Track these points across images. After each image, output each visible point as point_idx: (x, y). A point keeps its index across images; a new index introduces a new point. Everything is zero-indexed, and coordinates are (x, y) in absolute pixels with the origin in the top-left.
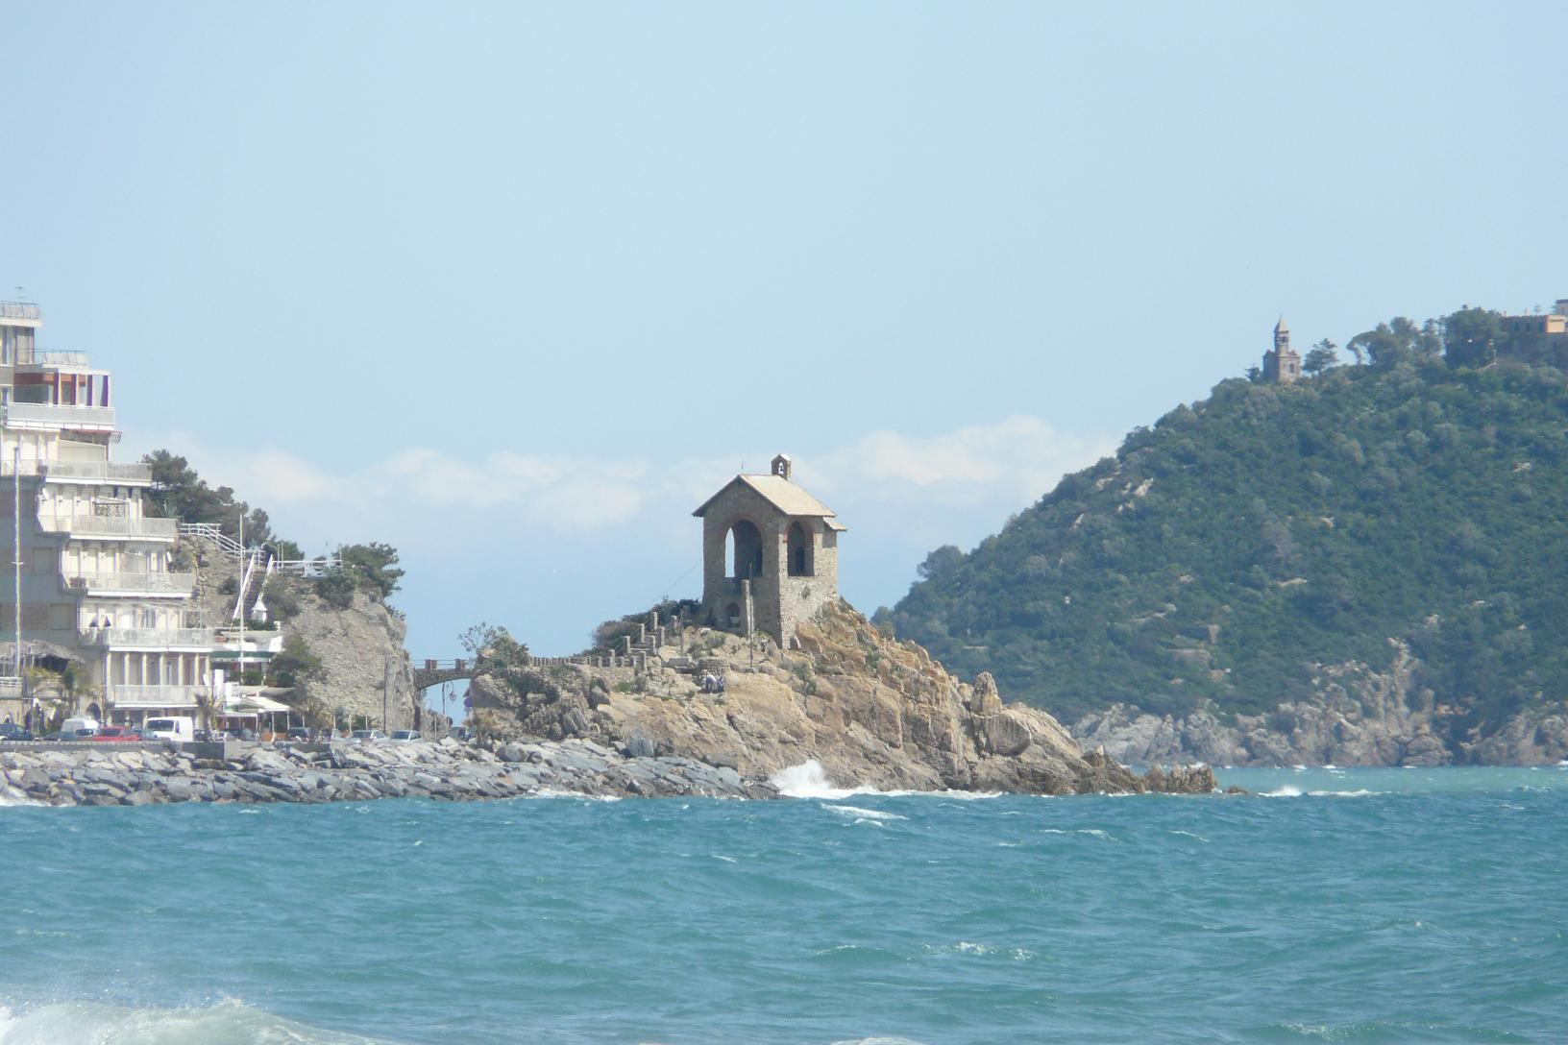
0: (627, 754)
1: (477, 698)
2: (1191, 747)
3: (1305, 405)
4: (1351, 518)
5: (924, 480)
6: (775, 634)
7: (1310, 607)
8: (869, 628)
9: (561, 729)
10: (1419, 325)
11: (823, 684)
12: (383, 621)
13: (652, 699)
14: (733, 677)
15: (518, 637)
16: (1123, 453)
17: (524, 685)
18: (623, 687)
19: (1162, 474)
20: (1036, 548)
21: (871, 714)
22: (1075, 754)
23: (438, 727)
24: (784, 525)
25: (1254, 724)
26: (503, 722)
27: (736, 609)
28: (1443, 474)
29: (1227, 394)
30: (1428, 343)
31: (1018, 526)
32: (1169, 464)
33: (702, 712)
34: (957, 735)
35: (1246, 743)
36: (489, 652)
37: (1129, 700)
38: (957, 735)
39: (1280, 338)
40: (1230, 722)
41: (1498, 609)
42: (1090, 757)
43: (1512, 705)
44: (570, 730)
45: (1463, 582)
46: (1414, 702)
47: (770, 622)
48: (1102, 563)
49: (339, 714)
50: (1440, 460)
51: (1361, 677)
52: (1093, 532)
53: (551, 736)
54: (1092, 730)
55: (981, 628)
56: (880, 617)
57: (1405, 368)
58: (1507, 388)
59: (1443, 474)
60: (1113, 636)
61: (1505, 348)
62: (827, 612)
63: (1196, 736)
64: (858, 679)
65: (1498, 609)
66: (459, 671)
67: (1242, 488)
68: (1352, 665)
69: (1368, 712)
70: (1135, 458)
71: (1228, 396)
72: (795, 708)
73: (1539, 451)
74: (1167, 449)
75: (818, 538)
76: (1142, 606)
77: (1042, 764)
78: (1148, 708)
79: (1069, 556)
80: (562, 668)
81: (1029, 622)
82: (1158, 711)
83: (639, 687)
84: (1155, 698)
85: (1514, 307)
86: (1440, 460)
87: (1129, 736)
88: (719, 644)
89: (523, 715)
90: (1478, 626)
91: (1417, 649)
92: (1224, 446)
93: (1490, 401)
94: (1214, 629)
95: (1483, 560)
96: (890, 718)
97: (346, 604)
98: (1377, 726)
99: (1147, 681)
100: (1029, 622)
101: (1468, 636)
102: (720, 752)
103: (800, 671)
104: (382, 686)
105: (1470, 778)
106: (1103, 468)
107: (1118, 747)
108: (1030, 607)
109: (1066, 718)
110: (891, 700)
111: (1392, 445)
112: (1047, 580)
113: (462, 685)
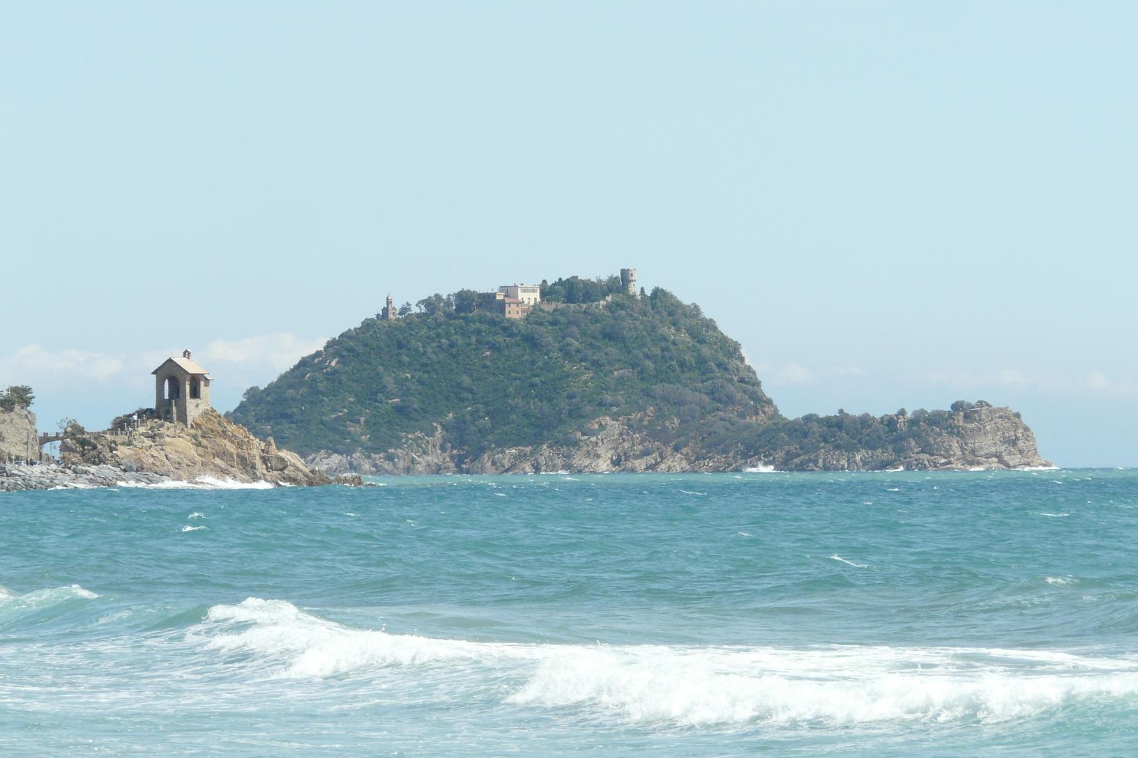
0: (125, 471)
1: (64, 448)
2: (352, 467)
3: (399, 329)
4: (418, 374)
5: (246, 356)
6: (185, 423)
7: (400, 410)
8: (222, 419)
9: (98, 460)
10: (445, 297)
11: (204, 442)
12: (26, 417)
13: (138, 447)
14: (168, 439)
15: (81, 423)
16: (326, 348)
17: (83, 443)
18: (123, 444)
19: (342, 357)
20: (290, 387)
21: (223, 454)
22: (307, 470)
23: (49, 460)
24: (189, 377)
25: (379, 457)
26: (75, 458)
27: (169, 412)
28: (454, 356)
29: (368, 324)
30: (448, 303)
31: (283, 378)
32: (345, 353)
33: (156, 454)
34: (258, 463)
35: (375, 465)
36: (69, 429)
37: (328, 448)
38: (258, 463)
39: (389, 302)
40: (369, 457)
41: (477, 411)
42: (313, 471)
43: (483, 450)
44: (101, 461)
45: (463, 400)
46: (443, 449)
47: (183, 417)
48: (319, 392)
49: (9, 454)
50: (454, 351)
51: (422, 439)
52: (314, 380)
53: (94, 463)
54: (313, 460)
55: (268, 419)
56: (227, 415)
57: (440, 315)
58: (481, 322)
59: (454, 356)
60: (322, 422)
61: (479, 306)
62: (206, 413)
63: (355, 463)
64: (218, 440)
65: (477, 411)
66: (57, 438)
67: (374, 363)
68: (418, 434)
69: (425, 453)
70: (331, 350)
71: (368, 325)
72: (192, 452)
73: (493, 347)
74: (342, 346)
75: (202, 383)
76: (333, 410)
77: (293, 474)
78: (336, 451)
79: (303, 390)
80: (98, 436)
81: (285, 416)
82: (340, 453)
83: (130, 444)
84: (340, 447)
85: (482, 288)
86: (454, 351)
87: (327, 463)
88: (162, 426)
89: (83, 455)
90: (469, 418)
91: (444, 427)
92: (366, 345)
93: (473, 327)
94: (362, 419)
95: (471, 391)
96: (231, 455)
97: (11, 410)
98: (429, 458)
99: (336, 440)
100: (285, 416)
101: (465, 423)
102: (163, 469)
103: (195, 437)
104: (26, 444)
105: (468, 479)
106: (318, 354)
107: (324, 468)
108: (288, 411)
109: (303, 455)
110: (232, 448)
111: (434, 345)
112: (293, 399)
113: (59, 443)
